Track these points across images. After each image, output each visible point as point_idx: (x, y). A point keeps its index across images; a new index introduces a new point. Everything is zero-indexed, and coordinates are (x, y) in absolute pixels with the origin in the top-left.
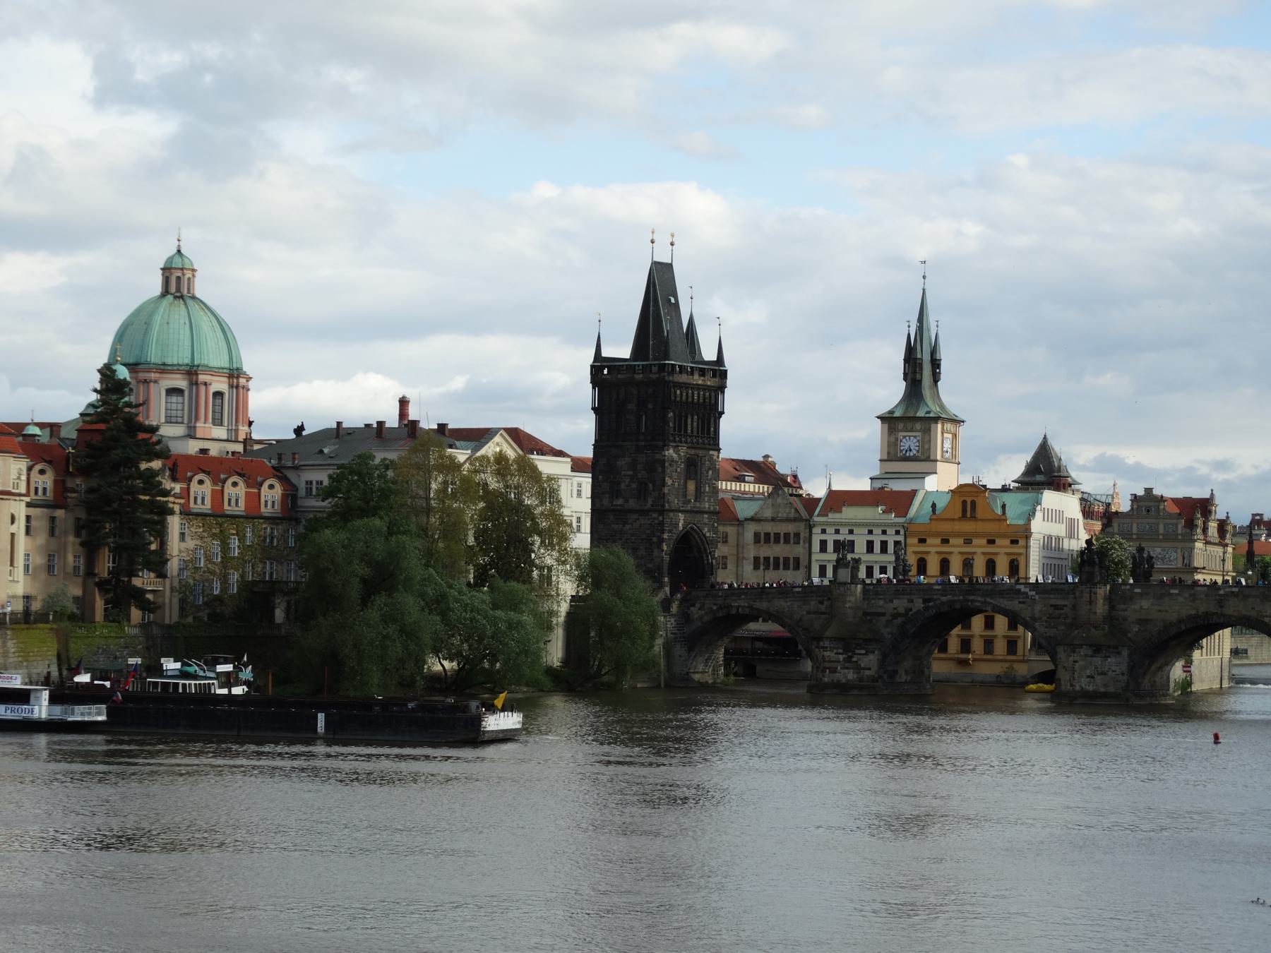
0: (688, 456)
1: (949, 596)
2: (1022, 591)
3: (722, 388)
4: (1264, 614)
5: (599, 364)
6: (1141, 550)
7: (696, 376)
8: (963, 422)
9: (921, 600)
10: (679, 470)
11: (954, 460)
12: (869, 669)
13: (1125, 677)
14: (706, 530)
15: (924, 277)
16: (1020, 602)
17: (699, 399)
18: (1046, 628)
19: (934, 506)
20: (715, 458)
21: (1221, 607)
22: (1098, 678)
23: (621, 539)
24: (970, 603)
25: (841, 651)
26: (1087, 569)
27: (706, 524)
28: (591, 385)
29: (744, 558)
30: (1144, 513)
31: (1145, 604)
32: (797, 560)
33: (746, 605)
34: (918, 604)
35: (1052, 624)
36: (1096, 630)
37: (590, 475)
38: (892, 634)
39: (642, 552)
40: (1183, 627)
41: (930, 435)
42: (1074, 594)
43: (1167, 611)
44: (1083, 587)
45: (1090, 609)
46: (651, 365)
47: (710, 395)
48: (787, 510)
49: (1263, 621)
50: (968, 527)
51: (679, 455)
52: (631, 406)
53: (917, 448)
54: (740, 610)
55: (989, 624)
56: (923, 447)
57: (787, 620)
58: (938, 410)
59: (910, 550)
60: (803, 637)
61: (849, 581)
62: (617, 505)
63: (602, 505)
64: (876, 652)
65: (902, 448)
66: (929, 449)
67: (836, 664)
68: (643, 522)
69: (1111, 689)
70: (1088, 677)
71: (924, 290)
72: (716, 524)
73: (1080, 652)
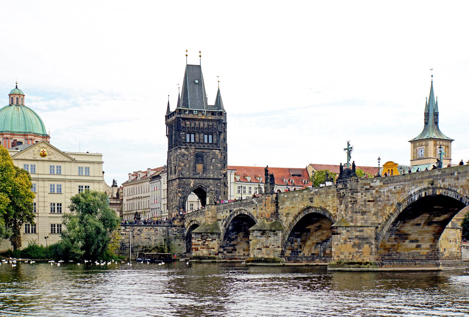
8: (453, 140)
10: (189, 159)
12: (214, 248)
20: (217, 153)
22: (264, 250)
25: (200, 239)
27: (211, 184)
40: (301, 218)
47: (213, 124)
64: (217, 239)
66: (428, 153)
69: (272, 257)
70: (258, 249)
73: (253, 235)
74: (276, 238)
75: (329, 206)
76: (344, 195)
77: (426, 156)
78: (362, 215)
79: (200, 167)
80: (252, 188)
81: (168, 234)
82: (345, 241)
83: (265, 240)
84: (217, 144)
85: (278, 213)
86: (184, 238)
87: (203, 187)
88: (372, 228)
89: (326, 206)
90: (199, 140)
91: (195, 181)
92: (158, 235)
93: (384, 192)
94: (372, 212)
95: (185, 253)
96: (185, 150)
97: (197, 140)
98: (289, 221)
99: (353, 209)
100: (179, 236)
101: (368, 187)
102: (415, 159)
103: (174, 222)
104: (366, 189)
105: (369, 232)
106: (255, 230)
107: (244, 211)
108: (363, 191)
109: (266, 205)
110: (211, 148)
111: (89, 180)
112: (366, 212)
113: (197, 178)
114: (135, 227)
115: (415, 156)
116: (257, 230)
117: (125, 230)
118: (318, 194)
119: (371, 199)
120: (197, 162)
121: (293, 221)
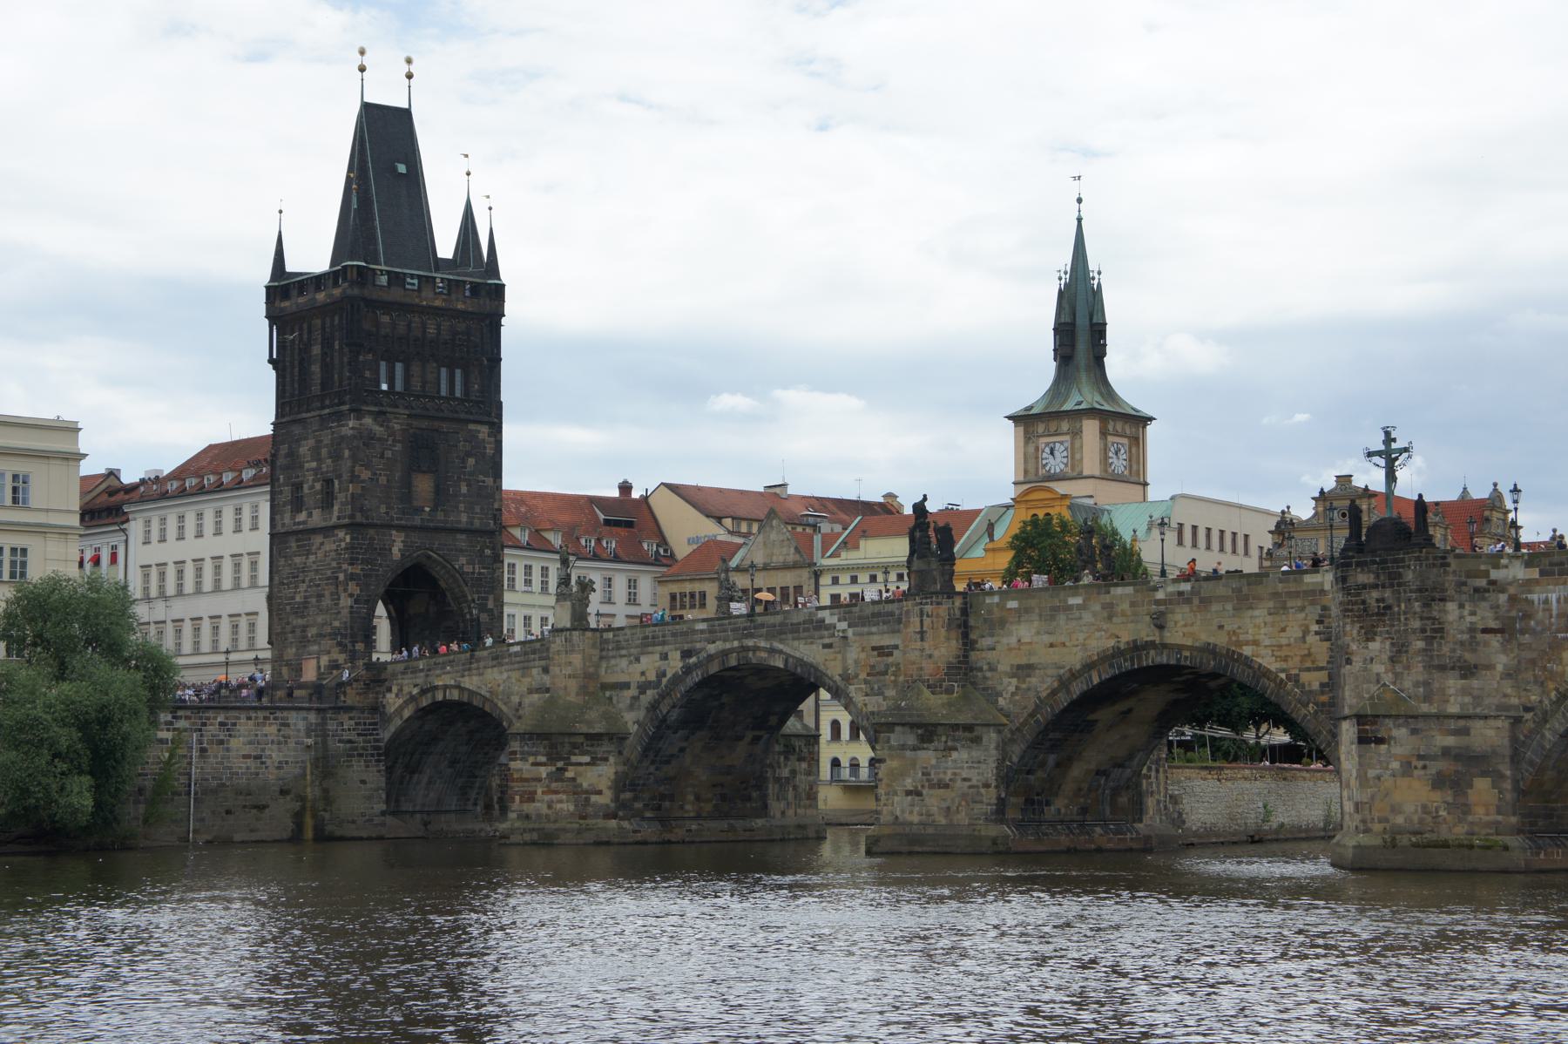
0: (411, 431)
2: (827, 622)
4: (1242, 637)
5: (276, 284)
8: (1151, 419)
9: (679, 652)
10: (388, 454)
11: (1133, 479)
12: (600, 793)
15: (1079, 201)
16: (826, 646)
17: (439, 333)
18: (867, 695)
20: (481, 436)
21: (1161, 627)
23: (303, 582)
24: (751, 654)
25: (543, 759)
27: (461, 551)
28: (267, 321)
31: (1025, 632)
33: (452, 682)
34: (675, 664)
35: (876, 687)
36: (933, 693)
39: (327, 602)
40: (1096, 680)
41: (1081, 438)
43: (1064, 644)
44: (910, 603)
45: (922, 650)
49: (1240, 655)
52: (316, 350)
53: (1065, 460)
56: (1073, 458)
62: (299, 523)
63: (283, 525)
64: (612, 759)
65: (1044, 462)
66: (1082, 459)
67: (534, 784)
68: (327, 547)
70: (909, 793)
71: (1079, 220)
73: (888, 741)
74: (976, 753)
75: (1256, 643)
76: (1389, 607)
77: (1073, 469)
78: (1464, 677)
79: (423, 485)
80: (517, 567)
81: (325, 743)
82: (1407, 769)
83: (933, 762)
84: (482, 402)
85: (967, 663)
86: (379, 755)
87: (435, 561)
88: (1499, 723)
89: (1240, 644)
90: (423, 387)
91: (406, 537)
92: (292, 745)
93: (1546, 601)
94: (1500, 668)
95: (383, 813)
96: (375, 420)
97: (416, 385)
98: (1032, 694)
99: (1432, 657)
100: (364, 748)
101: (1482, 583)
103: (345, 693)
104: (1476, 590)
105: (1489, 735)
106: (898, 724)
107: (764, 655)
108: (1464, 597)
109: (929, 635)
110: (462, 416)
111: (18, 524)
112: (1476, 667)
113: (414, 528)
114: (211, 714)
115: (1032, 470)
116: (903, 725)
117: (171, 723)
118: (1196, 601)
119: (1493, 624)
121: (1054, 693)
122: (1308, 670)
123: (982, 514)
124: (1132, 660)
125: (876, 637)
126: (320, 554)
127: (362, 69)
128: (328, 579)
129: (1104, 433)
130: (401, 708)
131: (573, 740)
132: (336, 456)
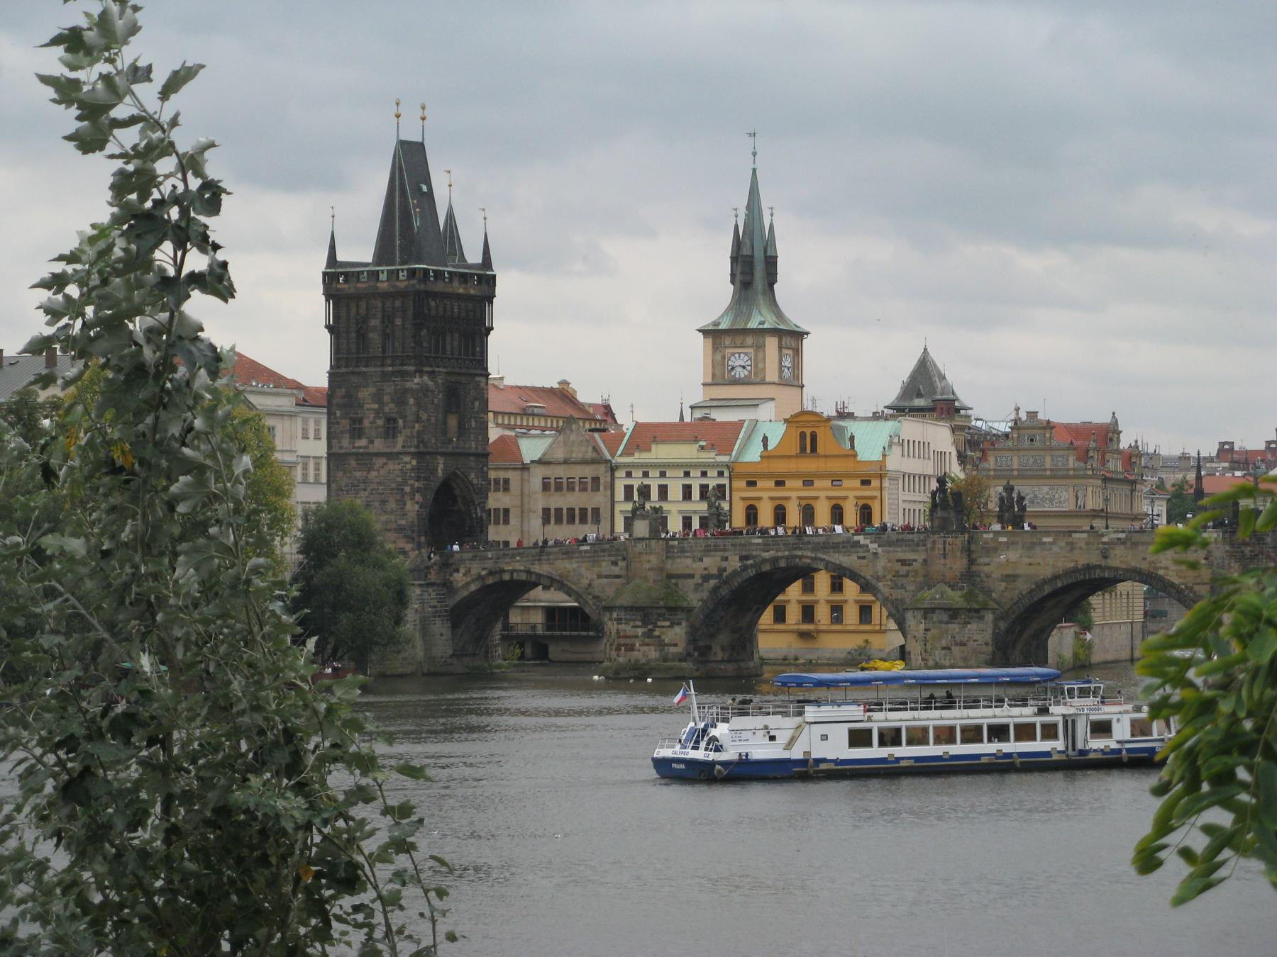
1: (772, 552)
3: (490, 298)
4: (1158, 565)
6: (1009, 489)
7: (456, 284)
8: (807, 333)
10: (436, 401)
12: (675, 645)
13: (990, 649)
14: (473, 475)
15: (754, 154)
16: (859, 558)
17: (459, 313)
19: (765, 440)
22: (956, 649)
23: (365, 490)
24: (797, 560)
25: (640, 624)
26: (940, 513)
27: (472, 468)
28: (323, 298)
29: (530, 510)
30: (1027, 443)
32: (596, 511)
33: (522, 568)
34: (734, 563)
37: (325, 410)
38: (702, 600)
39: (392, 505)
40: (1060, 584)
41: (764, 351)
42: (925, 545)
45: (945, 565)
46: (398, 270)
48: (584, 449)
50: (809, 465)
51: (435, 382)
52: (374, 322)
54: (515, 574)
55: (837, 587)
56: (756, 366)
57: (574, 587)
58: (774, 319)
59: (736, 496)
60: (594, 607)
61: (647, 536)
62: (360, 448)
63: (341, 448)
64: (684, 624)
70: (943, 648)
71: (754, 171)
72: (485, 469)
75: (1167, 568)
77: (756, 375)
83: (957, 630)
89: (1157, 568)
98: (1016, 592)
102: (720, 381)
116: (940, 609)
118: (1129, 544)
120: (448, 411)
121: (1032, 591)
122: (1198, 584)
123: (745, 425)
124: (1085, 574)
125: (900, 554)
126: (383, 472)
127: (398, 116)
128: (393, 489)
129: (780, 348)
130: (468, 584)
131: (659, 611)
132: (400, 401)
